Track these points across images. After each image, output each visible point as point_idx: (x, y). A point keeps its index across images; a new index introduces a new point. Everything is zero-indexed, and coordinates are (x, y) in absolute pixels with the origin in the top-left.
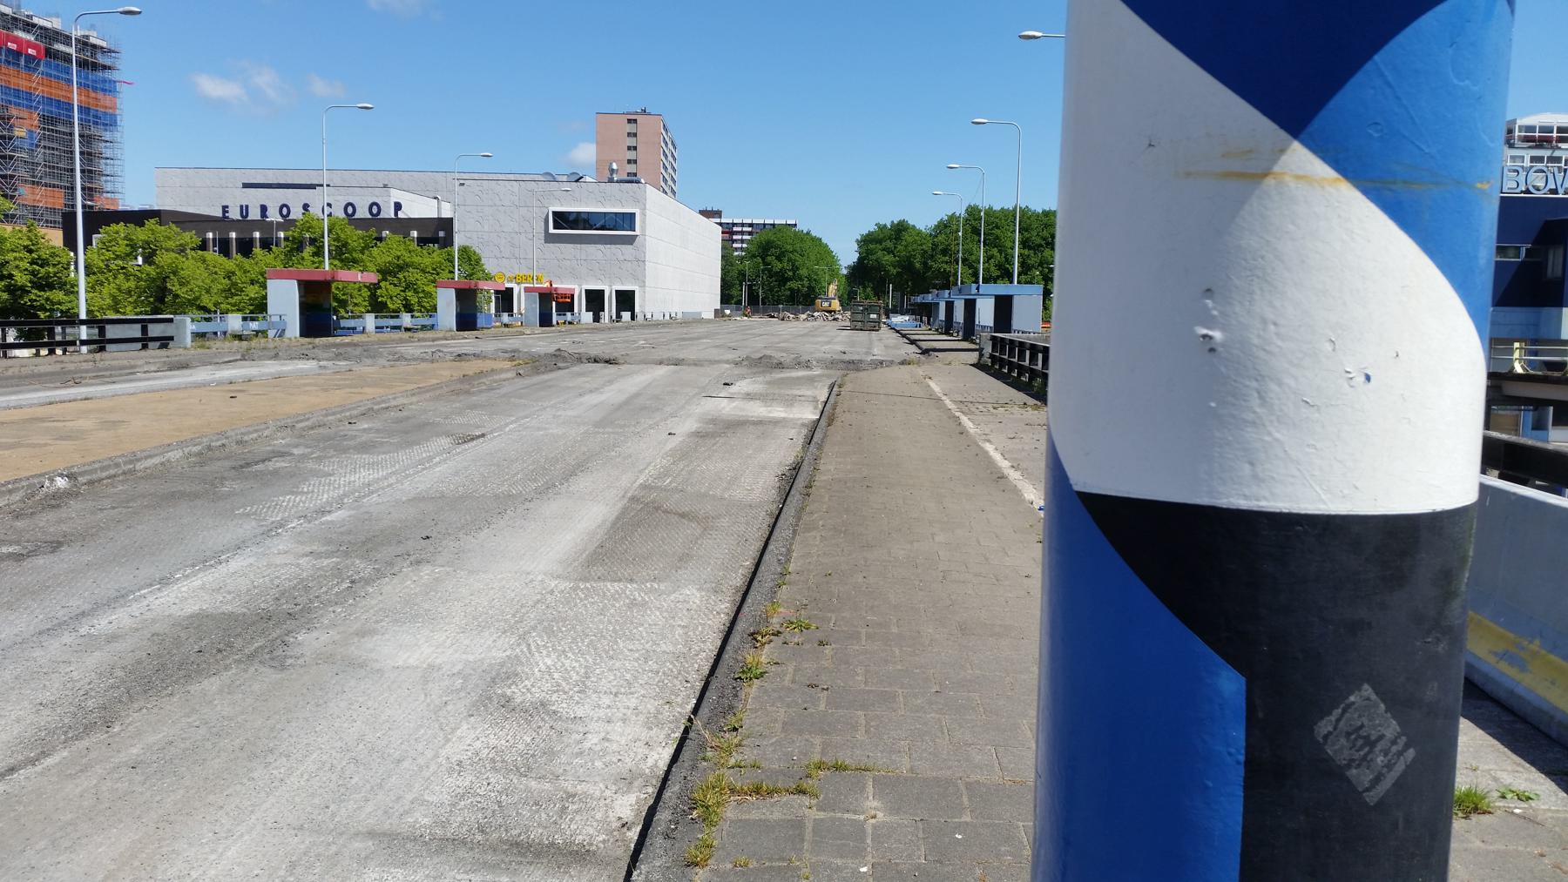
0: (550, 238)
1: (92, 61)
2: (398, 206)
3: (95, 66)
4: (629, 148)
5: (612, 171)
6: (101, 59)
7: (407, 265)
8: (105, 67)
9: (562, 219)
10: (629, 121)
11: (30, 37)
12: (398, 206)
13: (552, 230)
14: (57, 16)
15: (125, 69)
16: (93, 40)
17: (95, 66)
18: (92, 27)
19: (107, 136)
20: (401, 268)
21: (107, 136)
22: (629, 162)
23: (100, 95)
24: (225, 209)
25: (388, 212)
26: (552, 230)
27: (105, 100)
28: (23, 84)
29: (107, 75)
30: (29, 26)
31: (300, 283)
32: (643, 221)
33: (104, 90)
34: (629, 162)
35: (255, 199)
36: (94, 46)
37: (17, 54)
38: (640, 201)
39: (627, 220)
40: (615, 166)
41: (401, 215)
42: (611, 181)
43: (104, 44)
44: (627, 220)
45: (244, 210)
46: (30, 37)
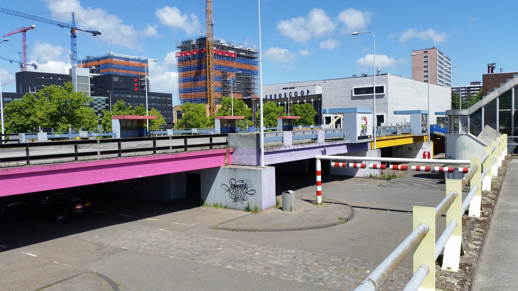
0: (353, 98)
1: (250, 57)
2: (308, 91)
3: (251, 58)
4: (425, 62)
5: (378, 71)
6: (255, 56)
7: (272, 111)
9: (358, 91)
10: (425, 52)
11: (233, 52)
12: (308, 91)
13: (354, 95)
16: (251, 50)
17: (251, 58)
18: (252, 46)
19: (255, 77)
21: (255, 77)
22: (425, 67)
23: (253, 66)
25: (305, 94)
26: (354, 95)
28: (231, 65)
29: (255, 60)
30: (233, 49)
31: (120, 121)
32: (387, 89)
34: (425, 67)
35: (283, 92)
37: (229, 57)
38: (386, 82)
39: (380, 89)
40: (379, 70)
41: (309, 94)
42: (378, 75)
43: (254, 51)
44: (380, 89)
45: (271, 96)
46: (233, 52)
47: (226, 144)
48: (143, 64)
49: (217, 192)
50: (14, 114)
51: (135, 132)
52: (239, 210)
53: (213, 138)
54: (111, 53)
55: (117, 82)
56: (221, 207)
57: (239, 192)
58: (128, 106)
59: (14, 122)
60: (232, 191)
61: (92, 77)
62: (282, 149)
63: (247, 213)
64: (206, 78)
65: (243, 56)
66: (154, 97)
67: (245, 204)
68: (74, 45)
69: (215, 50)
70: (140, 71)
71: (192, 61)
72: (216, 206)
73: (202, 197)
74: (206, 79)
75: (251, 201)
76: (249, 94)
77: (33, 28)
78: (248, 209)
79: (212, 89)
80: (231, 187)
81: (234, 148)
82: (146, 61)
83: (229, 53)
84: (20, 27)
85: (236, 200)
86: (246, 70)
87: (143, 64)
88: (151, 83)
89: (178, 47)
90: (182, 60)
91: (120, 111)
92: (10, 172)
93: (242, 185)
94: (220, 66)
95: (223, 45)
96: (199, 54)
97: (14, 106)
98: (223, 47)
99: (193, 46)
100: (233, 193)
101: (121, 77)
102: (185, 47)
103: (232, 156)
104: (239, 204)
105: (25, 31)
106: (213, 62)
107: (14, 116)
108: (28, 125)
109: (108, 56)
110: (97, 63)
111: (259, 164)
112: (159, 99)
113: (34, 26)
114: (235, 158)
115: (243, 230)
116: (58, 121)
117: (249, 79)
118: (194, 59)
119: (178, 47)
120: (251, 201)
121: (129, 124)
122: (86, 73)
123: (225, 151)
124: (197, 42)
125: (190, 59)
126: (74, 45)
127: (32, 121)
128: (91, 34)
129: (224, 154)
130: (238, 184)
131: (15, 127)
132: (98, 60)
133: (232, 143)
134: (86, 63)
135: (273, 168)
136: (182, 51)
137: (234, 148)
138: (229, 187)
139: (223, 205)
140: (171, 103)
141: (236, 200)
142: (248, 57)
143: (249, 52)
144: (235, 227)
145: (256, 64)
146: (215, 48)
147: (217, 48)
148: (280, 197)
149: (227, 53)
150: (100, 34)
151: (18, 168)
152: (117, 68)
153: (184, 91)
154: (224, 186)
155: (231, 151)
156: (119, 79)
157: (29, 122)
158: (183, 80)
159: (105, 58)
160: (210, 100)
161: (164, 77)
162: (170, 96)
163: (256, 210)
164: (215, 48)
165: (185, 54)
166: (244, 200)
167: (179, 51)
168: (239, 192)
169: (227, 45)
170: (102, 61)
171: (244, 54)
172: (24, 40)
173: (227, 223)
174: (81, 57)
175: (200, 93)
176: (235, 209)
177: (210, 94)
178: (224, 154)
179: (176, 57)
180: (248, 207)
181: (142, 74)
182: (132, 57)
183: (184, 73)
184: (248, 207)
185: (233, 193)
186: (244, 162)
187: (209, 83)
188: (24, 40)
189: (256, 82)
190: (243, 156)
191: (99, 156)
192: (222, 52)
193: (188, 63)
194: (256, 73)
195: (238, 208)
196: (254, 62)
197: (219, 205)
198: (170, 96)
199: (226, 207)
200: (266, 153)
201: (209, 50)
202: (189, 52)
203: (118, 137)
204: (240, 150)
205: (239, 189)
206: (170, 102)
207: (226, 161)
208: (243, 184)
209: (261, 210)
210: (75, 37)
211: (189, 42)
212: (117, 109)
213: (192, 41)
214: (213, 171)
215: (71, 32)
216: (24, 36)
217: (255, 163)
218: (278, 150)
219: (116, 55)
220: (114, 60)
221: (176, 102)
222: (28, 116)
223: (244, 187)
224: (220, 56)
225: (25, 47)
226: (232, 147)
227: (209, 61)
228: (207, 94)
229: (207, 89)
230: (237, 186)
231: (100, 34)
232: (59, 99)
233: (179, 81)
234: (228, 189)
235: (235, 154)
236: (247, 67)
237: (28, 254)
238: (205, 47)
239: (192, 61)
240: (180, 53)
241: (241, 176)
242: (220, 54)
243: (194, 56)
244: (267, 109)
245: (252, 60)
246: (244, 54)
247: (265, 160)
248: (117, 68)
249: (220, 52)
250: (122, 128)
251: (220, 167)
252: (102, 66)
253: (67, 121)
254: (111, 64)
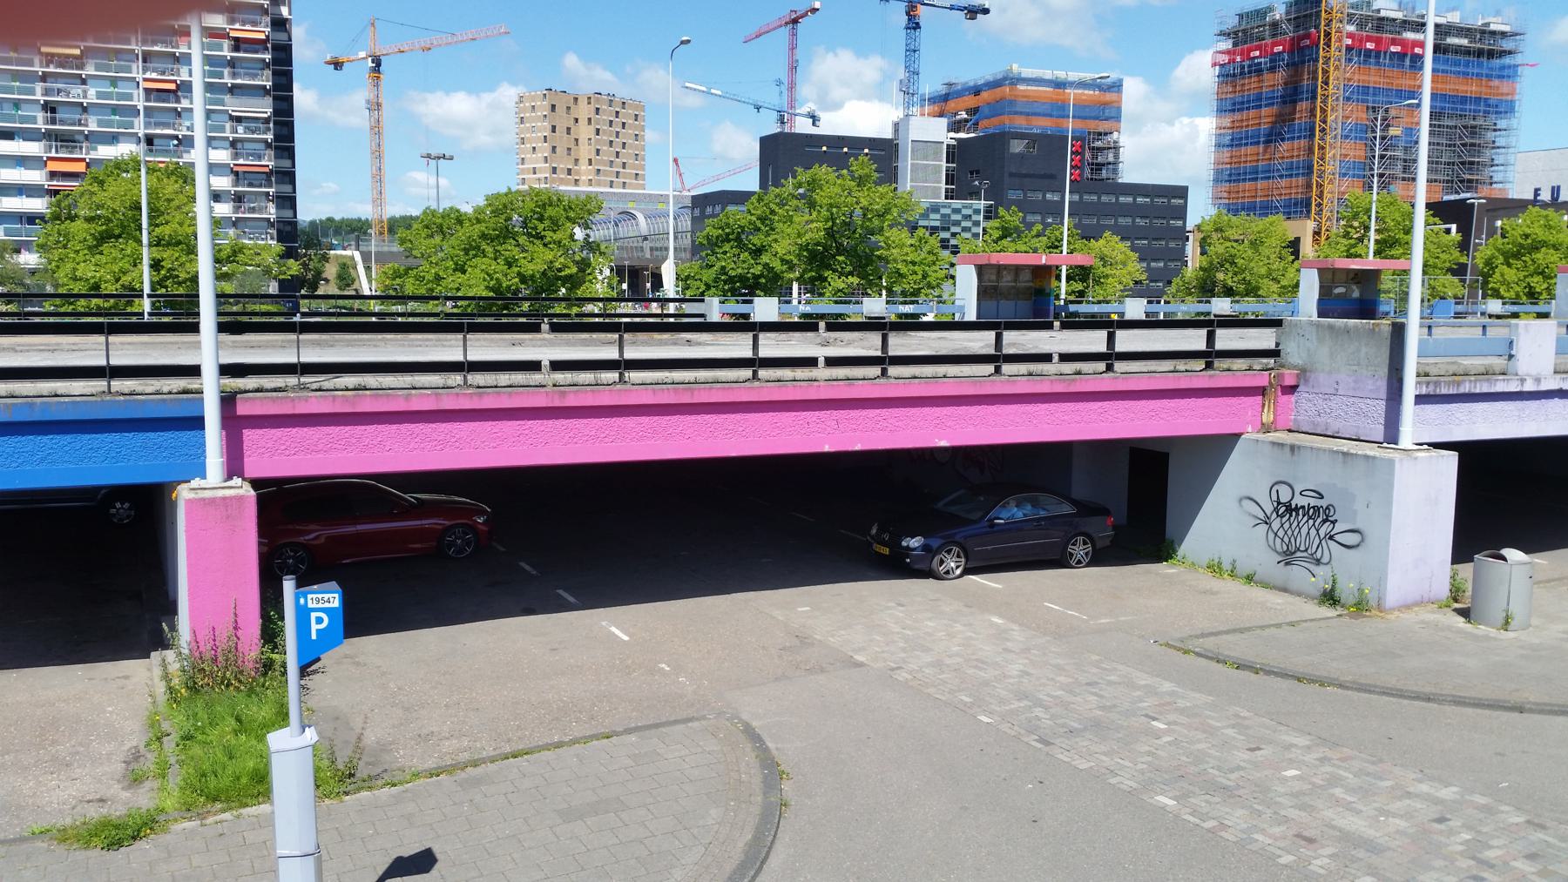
3: (1491, 54)
6: (1507, 45)
7: (1544, 244)
8: (1510, 53)
14: (1454, 9)
15: (1528, 53)
16: (1493, 27)
17: (1491, 54)
18: (1498, 13)
19: (1502, 124)
20: (1535, 247)
21: (1502, 124)
23: (1496, 82)
24: (1537, 191)
27: (1504, 87)
29: (1507, 60)
31: (981, 270)
33: (1501, 77)
36: (1493, 33)
37: (1401, 56)
47: (1274, 353)
48: (1109, 97)
49: (1223, 521)
50: (727, 247)
51: (1025, 305)
52: (1299, 595)
53: (1220, 333)
54: (1015, 67)
55: (1021, 156)
56: (1233, 574)
57: (1304, 530)
58: (1029, 226)
59: (723, 268)
60: (1276, 525)
61: (953, 142)
62: (1501, 387)
63: (1327, 612)
64: (1312, 130)
65: (1458, 50)
66: (1130, 199)
67: (1320, 578)
68: (912, 51)
69: (1350, 35)
70: (1096, 118)
71: (1266, 76)
72: (1215, 568)
73: (1168, 535)
74: (1312, 136)
75: (1345, 568)
76: (1470, 185)
77: (814, 10)
78: (1330, 597)
79: (1329, 168)
80: (1276, 510)
81: (1303, 372)
82: (1117, 86)
83: (1403, 43)
84: (784, 13)
85: (1288, 557)
86: (1464, 100)
87: (1109, 97)
88: (1124, 154)
89: (1222, 34)
90: (1228, 76)
91: (1005, 242)
92: (572, 401)
93: (1317, 509)
94: (1365, 90)
95: (1383, 14)
96: (1291, 52)
97: (728, 225)
98: (1381, 23)
99: (1275, 25)
100: (1281, 533)
101: (1033, 139)
102: (1244, 31)
103: (1293, 398)
104: (1298, 575)
105: (795, 21)
106: (1339, 73)
107: (725, 253)
108: (756, 277)
109: (1005, 79)
110: (971, 101)
111: (1392, 436)
112: (1145, 204)
113: (817, 5)
114: (1303, 407)
115: (1276, 674)
116: (828, 267)
117: (1473, 131)
118: (1272, 69)
119: (1222, 34)
120: (1345, 568)
121: (1007, 280)
122: (937, 131)
123: (1262, 380)
124: (1288, 13)
125: (1259, 71)
126: (912, 51)
127: (766, 265)
128: (962, 14)
129: (1261, 391)
130: (1299, 501)
131: (725, 282)
132: (977, 91)
133: (1294, 353)
134: (942, 102)
135: (1452, 458)
136: (1235, 45)
137: (1303, 372)
138: (1269, 509)
139: (1243, 569)
140: (1183, 217)
141: (1288, 557)
142: (1480, 53)
143: (1485, 33)
144: (1249, 656)
145: (1509, 73)
146: (1351, 28)
147: (1361, 26)
148: (1466, 570)
149: (1394, 42)
150: (986, 11)
151: (510, 394)
152: (1028, 114)
153: (1230, 176)
154: (1247, 503)
155: (1289, 381)
156: (1027, 146)
157: (757, 270)
158: (1232, 141)
159: (995, 84)
160: (1319, 205)
161: (1172, 136)
162: (1182, 192)
163: (1361, 606)
164: (1351, 28)
165: (1246, 54)
166: (1318, 562)
167: (1227, 45)
168: (1304, 530)
169: (1399, 15)
170: (985, 95)
171: (1465, 42)
172: (793, 48)
173: (1229, 637)
174: (930, 84)
175: (1284, 182)
176: (1285, 590)
177: (1320, 186)
178: (1261, 391)
179: (1214, 65)
180: (1333, 590)
181: (1103, 126)
182: (1073, 76)
183: (1237, 116)
184: (1333, 590)
185: (1281, 533)
186: (1335, 426)
187: (1322, 148)
188: (793, 48)
189: (1500, 142)
190: (1335, 402)
191: (821, 372)
192: (1378, 41)
193: (1251, 83)
194: (1508, 109)
195: (1294, 586)
196: (1503, 68)
197: (1226, 566)
198: (1182, 192)
199: (1250, 578)
200: (1420, 399)
201: (1328, 34)
202: (1258, 48)
203: (971, 316)
204: (1323, 380)
205: (1303, 520)
206: (1181, 213)
207: (1268, 417)
208: (1319, 503)
209: (1380, 607)
210: (918, 26)
211: (1260, 14)
212: (996, 234)
213: (1270, 9)
214: (1219, 447)
215: (908, 14)
216: (794, 35)
217: (1378, 432)
218: (1483, 387)
219: (1027, 72)
220: (1021, 87)
221: (1200, 209)
222: (758, 252)
223: (1322, 514)
224: (1368, 53)
225: (793, 68)
226: (1295, 367)
227: (1325, 72)
228: (1309, 186)
229: (1310, 168)
230: (1297, 509)
231: (986, 11)
232: (831, 206)
233: (1218, 145)
234: (1261, 515)
235: (1303, 394)
236: (1472, 89)
237: (613, 629)
238: (1317, 27)
239: (1266, 76)
240: (1228, 52)
241: (1311, 476)
242: (1370, 46)
243: (1275, 58)
244: (1527, 236)
245: (1496, 62)
246: (1465, 42)
247: (1416, 423)
248: (1028, 114)
249: (1369, 39)
250: (984, 293)
251: (1238, 436)
252: (986, 111)
253: (849, 268)
254: (1012, 102)
